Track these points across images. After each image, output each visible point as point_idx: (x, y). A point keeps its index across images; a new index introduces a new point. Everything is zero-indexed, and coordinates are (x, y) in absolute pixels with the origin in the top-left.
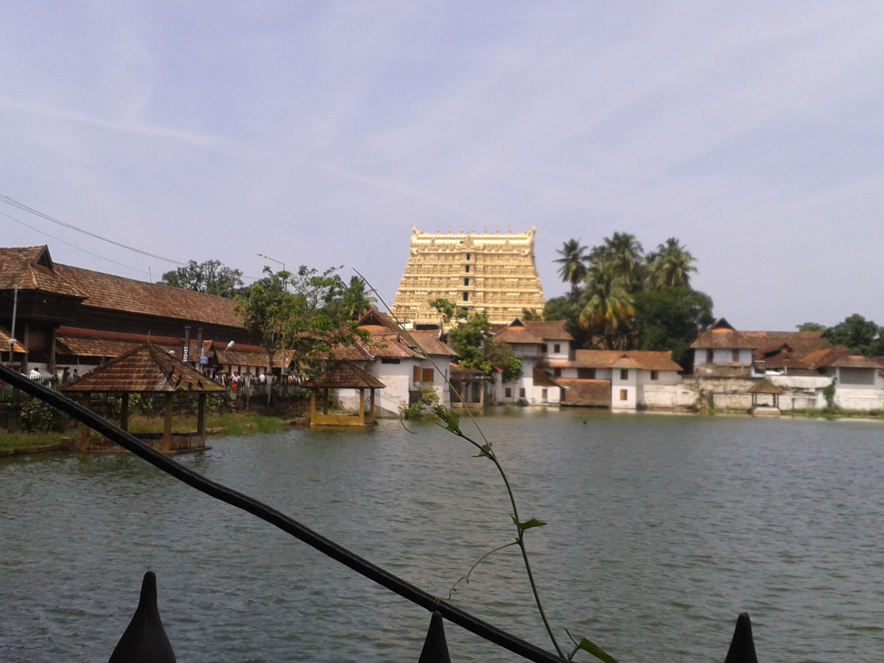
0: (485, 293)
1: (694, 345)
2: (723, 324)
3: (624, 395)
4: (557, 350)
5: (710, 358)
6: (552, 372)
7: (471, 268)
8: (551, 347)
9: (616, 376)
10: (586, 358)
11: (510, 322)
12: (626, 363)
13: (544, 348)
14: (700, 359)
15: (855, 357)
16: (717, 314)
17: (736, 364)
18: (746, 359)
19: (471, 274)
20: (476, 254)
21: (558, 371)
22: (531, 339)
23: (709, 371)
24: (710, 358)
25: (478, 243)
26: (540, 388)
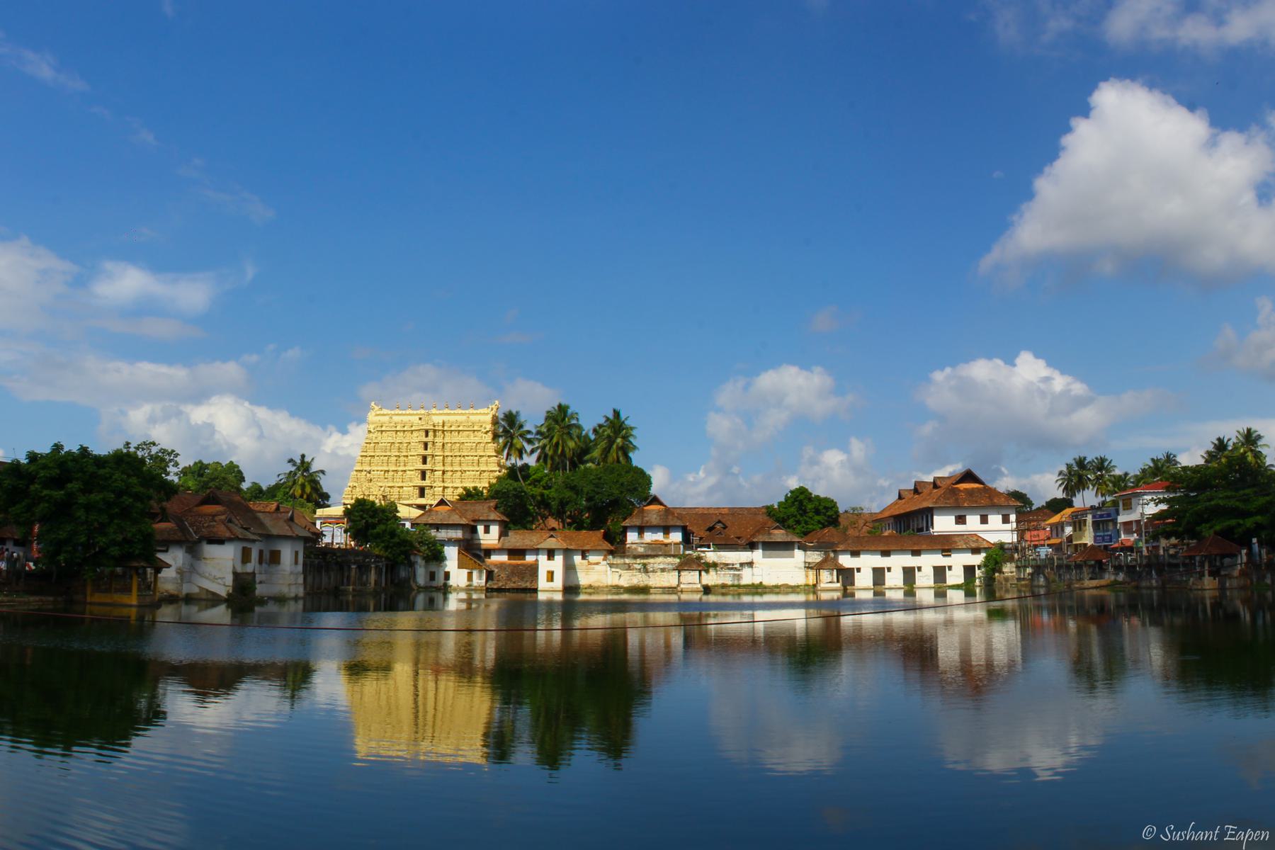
0: (444, 472)
1: (627, 523)
2: (655, 500)
3: (551, 576)
4: (487, 531)
6: (482, 554)
7: (430, 446)
9: (542, 559)
10: (517, 539)
11: (435, 503)
12: (551, 543)
13: (474, 530)
14: (632, 537)
15: (776, 532)
16: (654, 490)
17: (666, 541)
18: (676, 537)
19: (429, 452)
20: (435, 431)
21: (488, 552)
22: (456, 519)
23: (641, 550)
25: (438, 420)
26: (465, 572)
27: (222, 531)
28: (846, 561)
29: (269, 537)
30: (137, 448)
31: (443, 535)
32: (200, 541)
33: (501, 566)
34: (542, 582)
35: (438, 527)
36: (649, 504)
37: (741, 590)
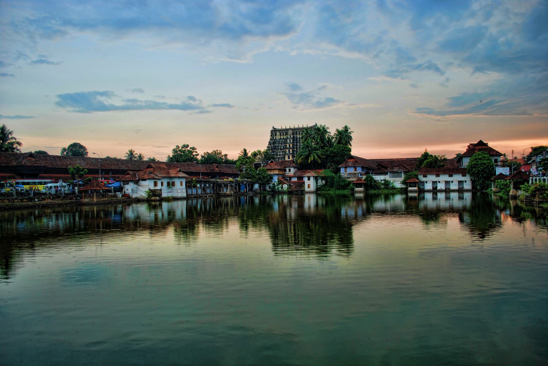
1: (340, 166)
3: (309, 187)
4: (290, 170)
5: (346, 171)
8: (287, 169)
13: (285, 170)
17: (356, 172)
21: (290, 178)
24: (346, 171)
27: (146, 176)
28: (421, 178)
29: (171, 178)
30: (182, 148)
31: (272, 173)
32: (139, 180)
33: (295, 182)
34: (307, 189)
35: (270, 170)
36: (350, 159)
37: (395, 191)
